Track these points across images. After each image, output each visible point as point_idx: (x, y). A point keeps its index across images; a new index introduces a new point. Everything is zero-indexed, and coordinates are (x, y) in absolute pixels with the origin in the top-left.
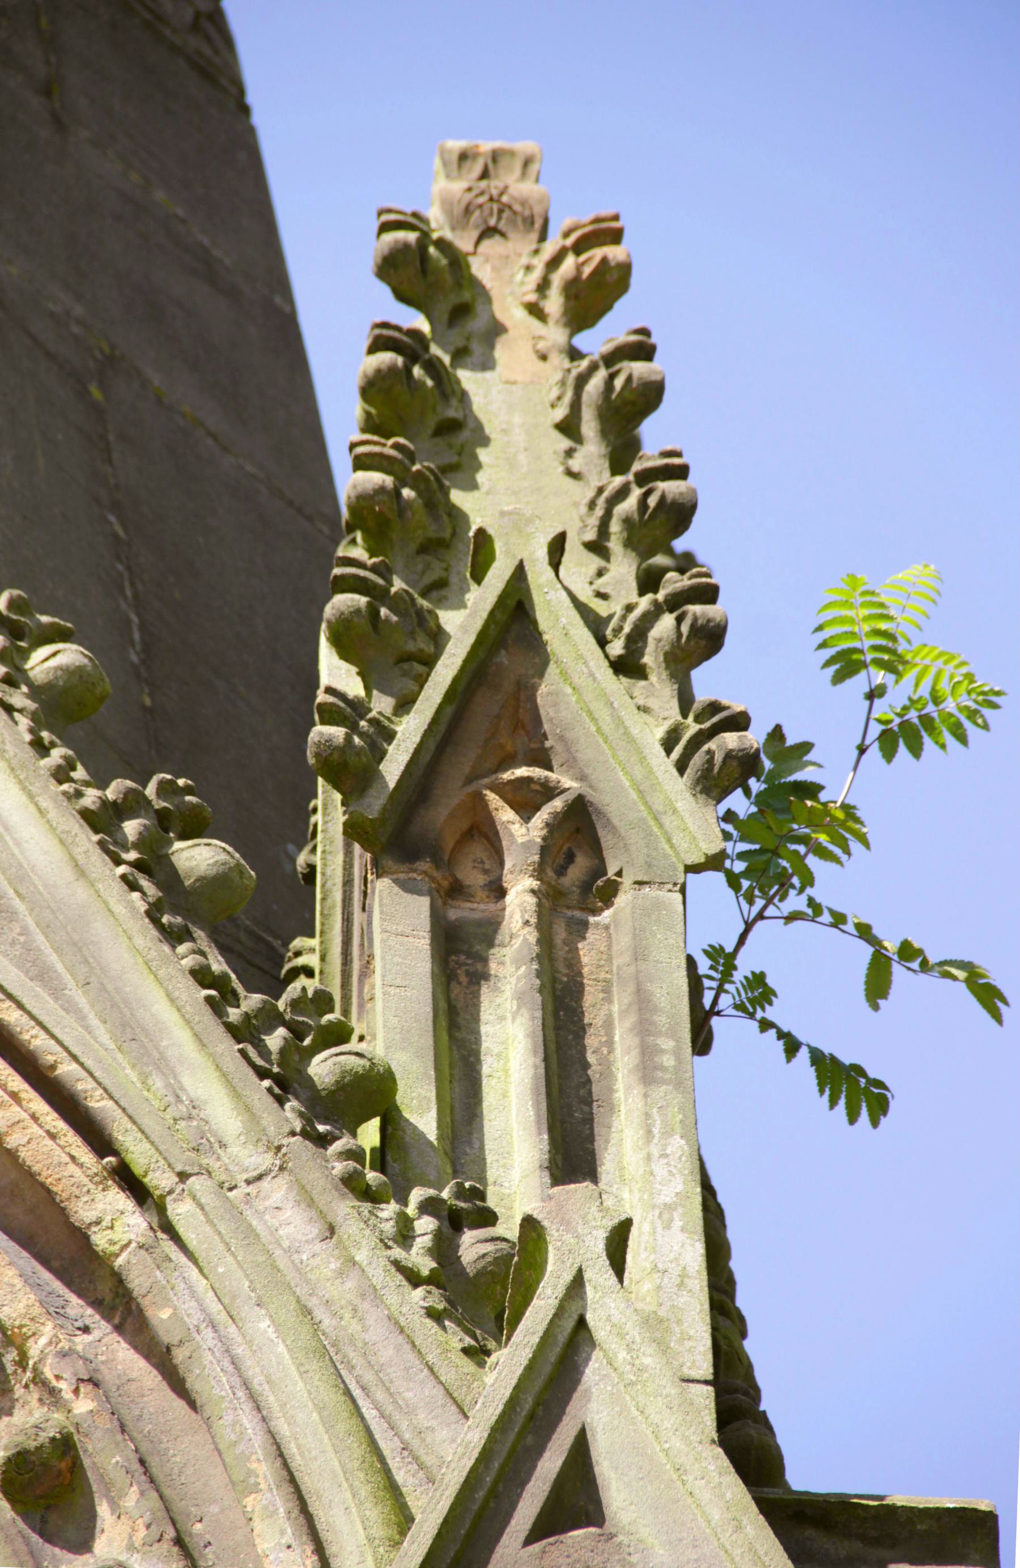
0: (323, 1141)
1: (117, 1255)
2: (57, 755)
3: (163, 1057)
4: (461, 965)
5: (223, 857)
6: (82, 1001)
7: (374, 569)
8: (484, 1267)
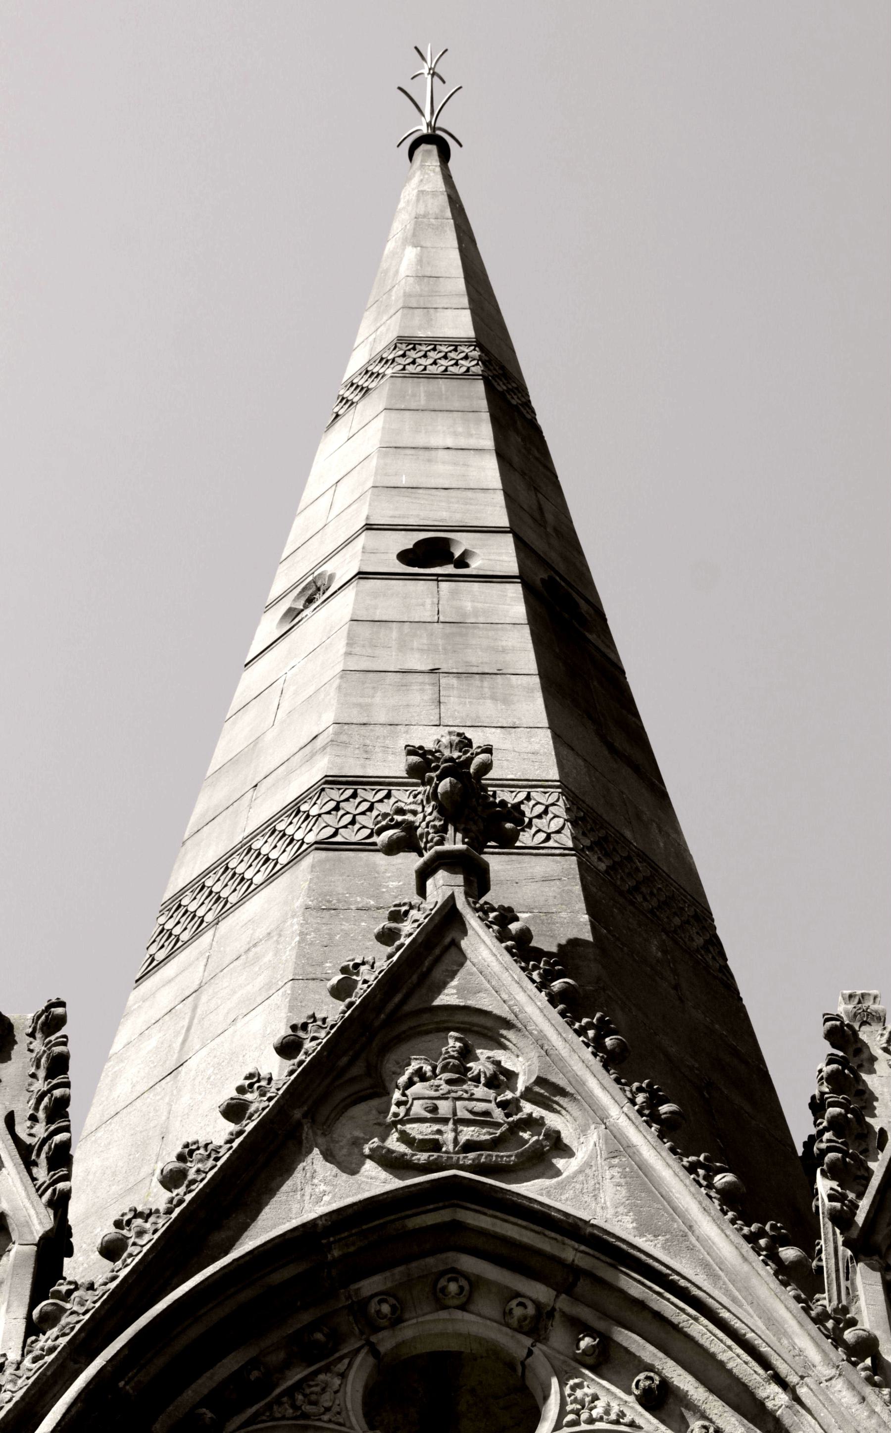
0: (855, 1364)
2: (730, 1214)
3: (785, 1331)
5: (799, 1253)
6: (751, 1311)
7: (842, 1143)
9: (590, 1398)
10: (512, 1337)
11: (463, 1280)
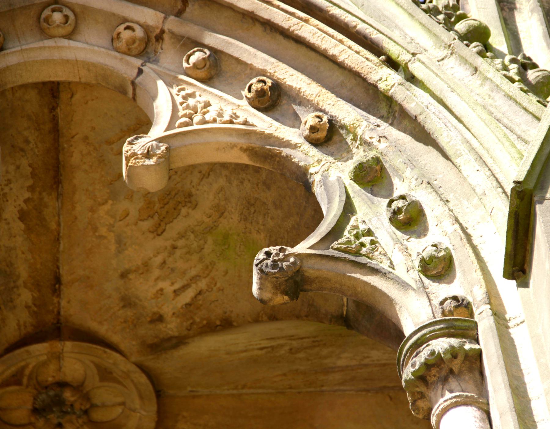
1: (390, 90)
4: (505, 6)
8: (539, 80)
9: (203, 104)
10: (121, 59)
11: (67, 10)
